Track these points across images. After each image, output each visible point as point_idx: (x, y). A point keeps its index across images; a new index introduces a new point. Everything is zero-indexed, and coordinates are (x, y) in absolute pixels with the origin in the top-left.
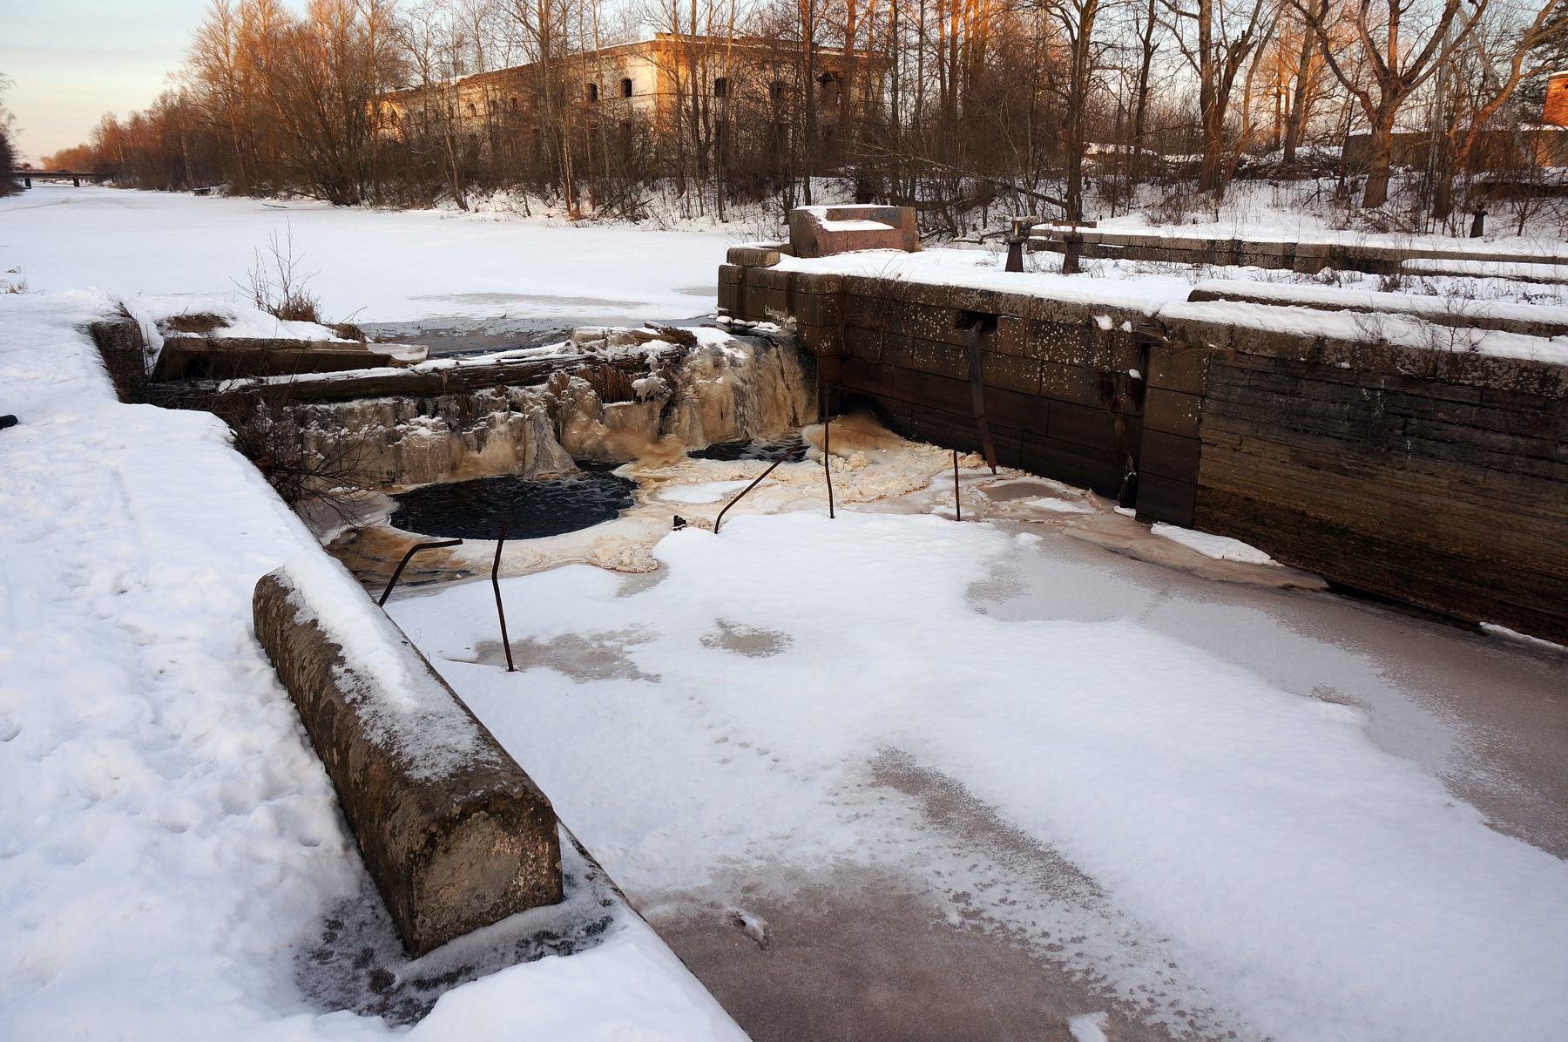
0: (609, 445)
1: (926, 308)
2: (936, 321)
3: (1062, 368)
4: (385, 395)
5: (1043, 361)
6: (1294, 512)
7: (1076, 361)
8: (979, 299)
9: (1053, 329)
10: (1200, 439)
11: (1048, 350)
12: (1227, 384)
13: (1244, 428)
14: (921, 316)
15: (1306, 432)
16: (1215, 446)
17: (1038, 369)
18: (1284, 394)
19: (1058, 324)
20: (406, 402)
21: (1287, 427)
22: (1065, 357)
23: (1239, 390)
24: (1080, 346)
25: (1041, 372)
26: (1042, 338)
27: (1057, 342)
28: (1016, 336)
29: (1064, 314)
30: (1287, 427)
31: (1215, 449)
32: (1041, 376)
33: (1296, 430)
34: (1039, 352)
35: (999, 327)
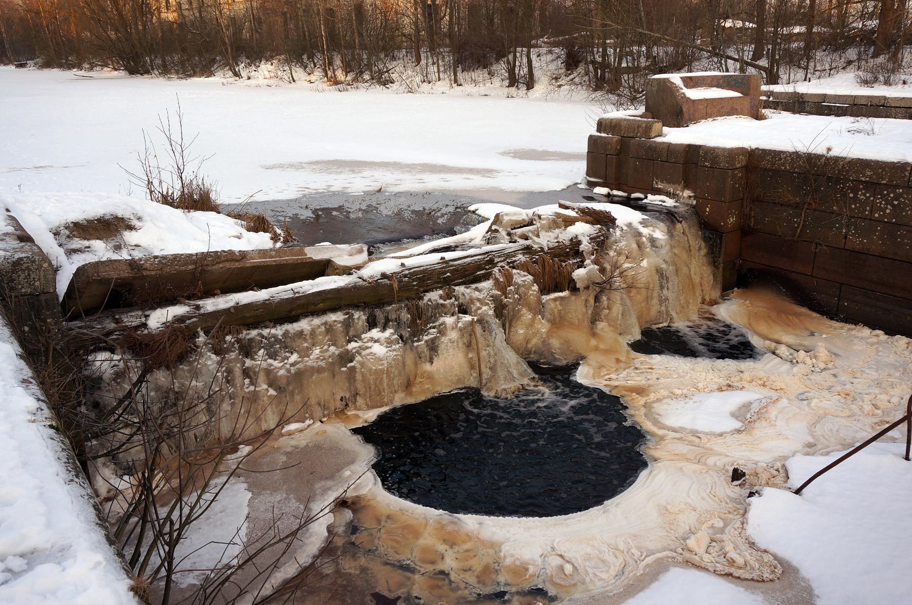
0: (555, 343)
1: (873, 186)
2: (886, 200)
4: (334, 310)
14: (864, 195)
20: (356, 316)
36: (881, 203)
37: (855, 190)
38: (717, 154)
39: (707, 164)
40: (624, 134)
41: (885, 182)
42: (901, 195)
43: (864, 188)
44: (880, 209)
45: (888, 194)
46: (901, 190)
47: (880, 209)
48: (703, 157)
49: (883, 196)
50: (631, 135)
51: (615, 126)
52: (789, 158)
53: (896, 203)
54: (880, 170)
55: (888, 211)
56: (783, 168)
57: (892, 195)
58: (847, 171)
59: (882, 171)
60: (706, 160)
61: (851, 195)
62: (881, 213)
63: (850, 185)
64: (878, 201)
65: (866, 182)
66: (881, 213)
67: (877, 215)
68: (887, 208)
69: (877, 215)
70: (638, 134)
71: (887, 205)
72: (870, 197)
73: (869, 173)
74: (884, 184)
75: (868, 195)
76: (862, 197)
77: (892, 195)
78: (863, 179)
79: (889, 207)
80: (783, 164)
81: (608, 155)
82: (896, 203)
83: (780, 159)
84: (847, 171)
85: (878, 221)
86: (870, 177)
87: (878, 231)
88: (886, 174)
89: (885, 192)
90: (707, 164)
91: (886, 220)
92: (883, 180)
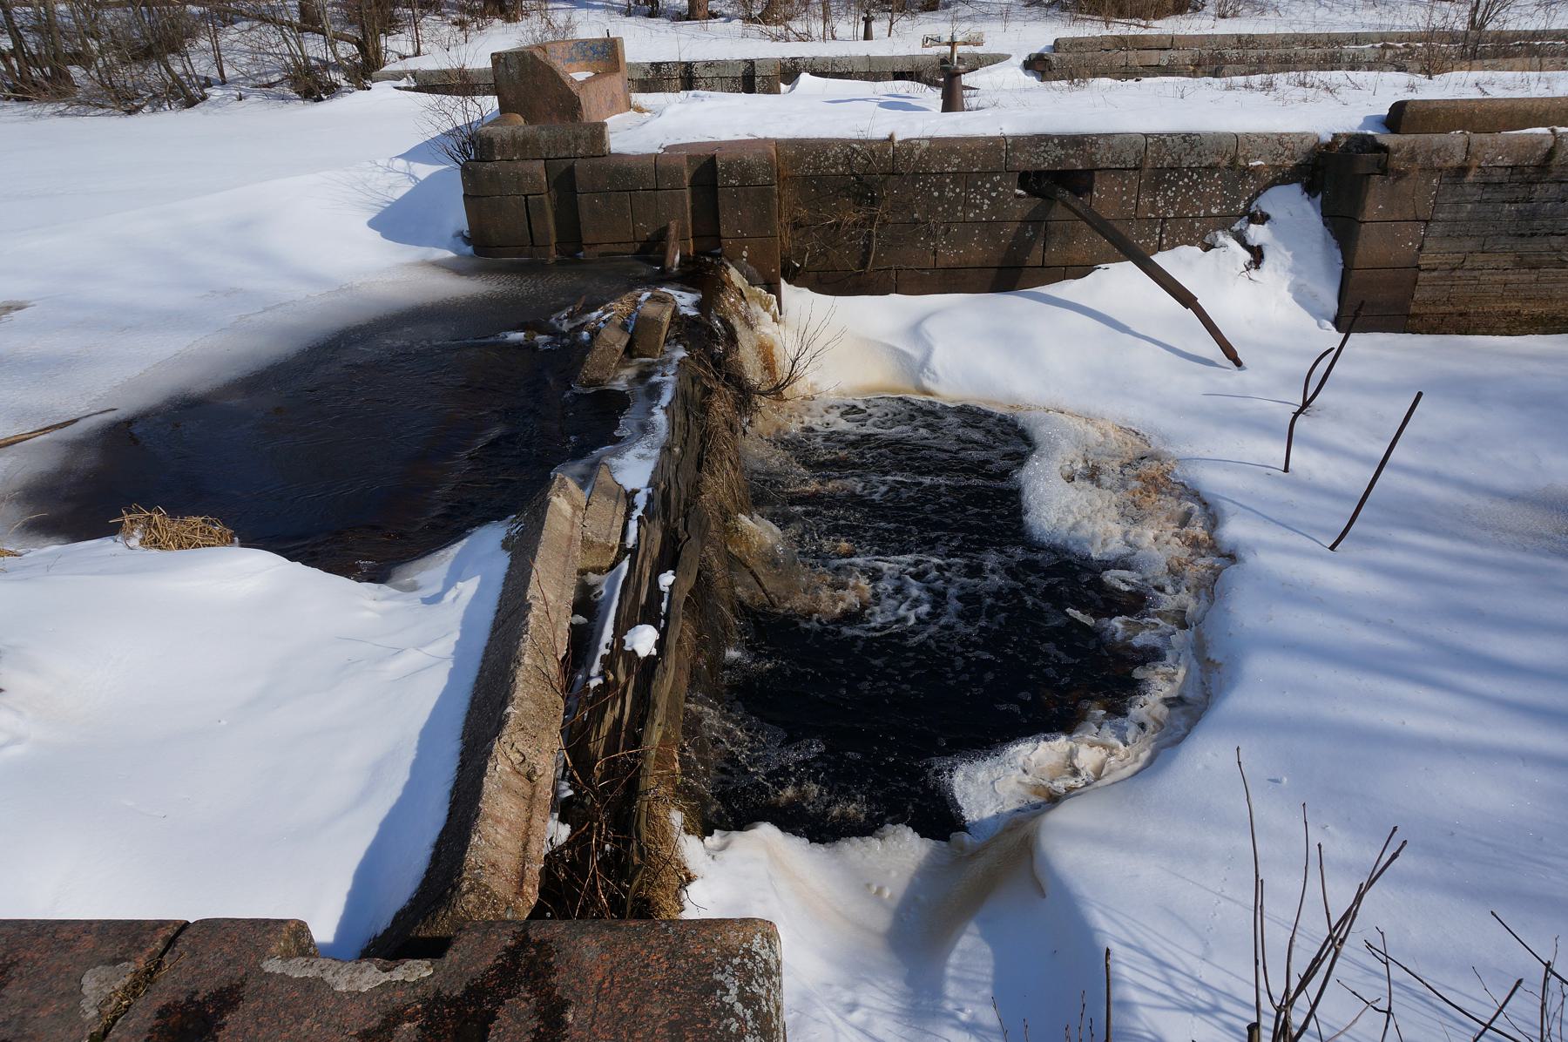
1: (963, 177)
3: (1193, 223)
5: (1165, 219)
6: (1509, 314)
7: (1215, 211)
8: (1060, 152)
9: (1181, 177)
10: (1418, 267)
11: (1173, 205)
12: (1457, 203)
13: (1469, 244)
14: (954, 191)
15: (1533, 235)
16: (1434, 270)
17: (1158, 230)
18: (1516, 202)
19: (1189, 168)
21: (1514, 235)
22: (1199, 209)
23: (1469, 206)
24: (1221, 191)
25: (1161, 233)
26: (1166, 190)
27: (1187, 192)
28: (1124, 193)
29: (1199, 155)
30: (1514, 235)
31: (1435, 274)
32: (1161, 238)
33: (1522, 235)
34: (1160, 208)
35: (1097, 185)
36: (975, 198)
37: (941, 187)
38: (748, 165)
39: (734, 182)
40: (547, 153)
41: (977, 169)
42: (999, 183)
43: (952, 182)
44: (976, 206)
45: (983, 185)
46: (998, 177)
47: (976, 206)
48: (723, 171)
49: (977, 188)
50: (565, 153)
51: (525, 142)
52: (840, 155)
53: (994, 194)
54: (970, 155)
55: (985, 207)
56: (833, 171)
57: (988, 186)
58: (927, 163)
59: (973, 155)
60: (730, 176)
61: (936, 194)
62: (977, 211)
63: (932, 180)
64: (971, 196)
65: (954, 173)
66: (977, 211)
67: (972, 215)
68: (983, 203)
69: (972, 215)
70: (580, 151)
71: (983, 199)
72: (960, 192)
73: (957, 161)
74: (976, 172)
75: (958, 190)
76: (951, 194)
77: (988, 186)
78: (950, 170)
79: (986, 201)
80: (835, 165)
81: (526, 196)
82: (994, 194)
83: (827, 159)
84: (927, 163)
85: (976, 222)
86: (958, 165)
87: (975, 235)
88: (978, 157)
89: (979, 183)
90: (734, 182)
91: (984, 219)
92: (974, 167)
